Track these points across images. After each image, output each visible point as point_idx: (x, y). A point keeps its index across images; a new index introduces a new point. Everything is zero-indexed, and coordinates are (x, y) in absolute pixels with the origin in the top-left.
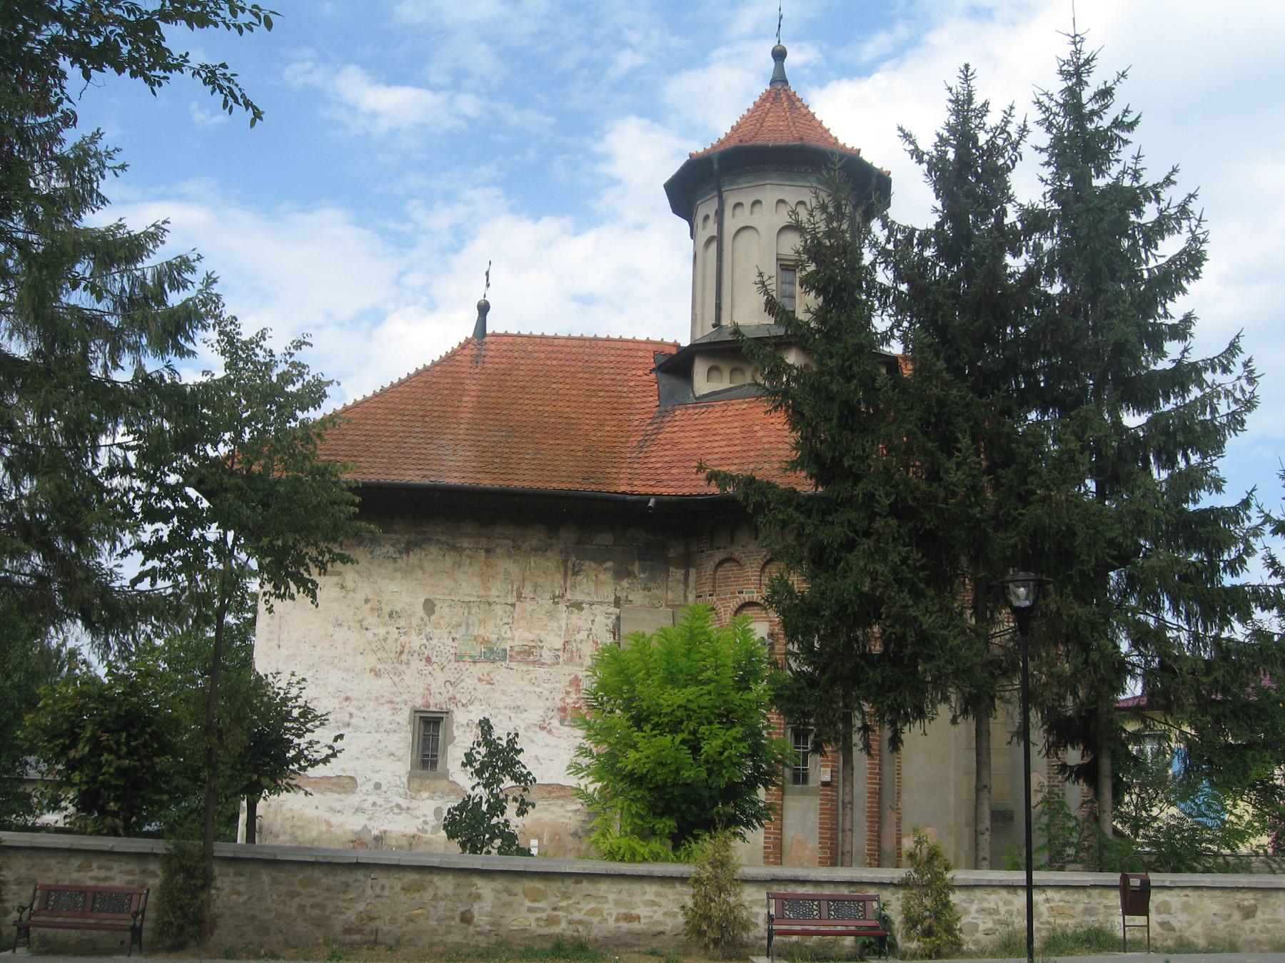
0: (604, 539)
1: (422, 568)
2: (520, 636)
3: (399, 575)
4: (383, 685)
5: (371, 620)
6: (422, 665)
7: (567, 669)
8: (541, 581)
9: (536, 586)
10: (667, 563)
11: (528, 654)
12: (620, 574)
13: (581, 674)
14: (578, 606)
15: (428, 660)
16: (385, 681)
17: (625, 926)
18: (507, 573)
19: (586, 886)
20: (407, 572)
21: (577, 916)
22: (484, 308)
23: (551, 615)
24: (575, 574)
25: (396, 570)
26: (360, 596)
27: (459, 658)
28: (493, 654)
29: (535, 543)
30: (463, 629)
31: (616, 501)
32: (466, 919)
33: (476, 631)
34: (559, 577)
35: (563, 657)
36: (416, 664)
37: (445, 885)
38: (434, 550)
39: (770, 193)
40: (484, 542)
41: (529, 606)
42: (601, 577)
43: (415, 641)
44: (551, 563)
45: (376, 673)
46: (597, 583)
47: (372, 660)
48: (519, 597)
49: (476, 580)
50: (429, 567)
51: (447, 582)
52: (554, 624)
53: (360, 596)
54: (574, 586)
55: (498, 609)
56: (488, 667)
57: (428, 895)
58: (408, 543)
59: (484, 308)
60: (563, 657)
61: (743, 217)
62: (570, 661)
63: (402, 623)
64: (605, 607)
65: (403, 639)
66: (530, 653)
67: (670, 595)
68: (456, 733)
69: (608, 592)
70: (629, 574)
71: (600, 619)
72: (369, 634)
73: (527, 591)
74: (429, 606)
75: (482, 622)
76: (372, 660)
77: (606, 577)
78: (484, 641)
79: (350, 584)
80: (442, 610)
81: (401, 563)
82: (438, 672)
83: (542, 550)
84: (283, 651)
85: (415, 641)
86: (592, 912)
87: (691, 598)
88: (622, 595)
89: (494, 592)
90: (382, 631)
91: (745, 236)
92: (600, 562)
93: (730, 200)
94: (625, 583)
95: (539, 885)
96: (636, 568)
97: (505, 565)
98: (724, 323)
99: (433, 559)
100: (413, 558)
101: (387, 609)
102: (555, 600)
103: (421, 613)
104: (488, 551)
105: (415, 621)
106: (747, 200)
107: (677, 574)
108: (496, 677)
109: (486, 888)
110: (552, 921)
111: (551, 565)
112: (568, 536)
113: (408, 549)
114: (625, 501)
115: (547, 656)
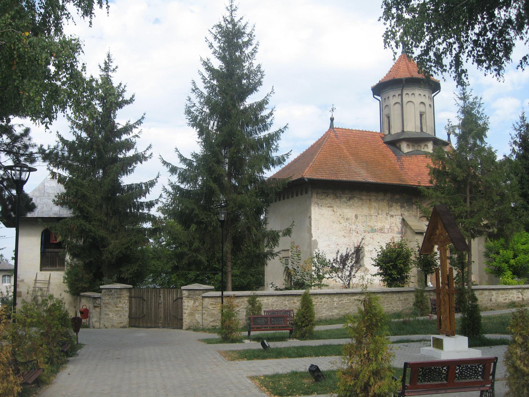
0: (397, 197)
1: (354, 205)
2: (379, 225)
3: (348, 207)
4: (346, 240)
5: (342, 221)
6: (356, 234)
7: (391, 234)
8: (383, 209)
9: (382, 210)
10: (412, 204)
11: (381, 230)
12: (402, 207)
13: (395, 235)
14: (392, 216)
15: (357, 232)
16: (347, 239)
17: (518, 299)
18: (375, 207)
19: (511, 291)
20: (350, 206)
21: (510, 298)
22: (332, 120)
23: (386, 219)
24: (391, 207)
25: (347, 206)
26: (338, 214)
27: (365, 232)
28: (373, 231)
29: (381, 198)
30: (365, 223)
31: (410, 187)
32: (491, 300)
33: (369, 224)
34: (387, 208)
35: (390, 231)
36: (355, 234)
37: (486, 293)
38: (356, 200)
39: (417, 92)
40: (368, 197)
41: (380, 216)
42: (398, 208)
43: (354, 227)
44: (385, 203)
45: (345, 237)
46: (397, 210)
47: (343, 233)
48: (378, 214)
49: (367, 209)
50: (356, 205)
51: (361, 210)
52: (387, 222)
53: (338, 214)
54: (391, 210)
55: (373, 217)
56: (372, 234)
57: (484, 296)
58: (350, 198)
59: (332, 120)
60: (390, 231)
61: (411, 98)
62: (391, 232)
63: (350, 222)
64: (399, 217)
65: (351, 226)
66: (382, 230)
67: (414, 213)
68: (366, 253)
69: (399, 212)
70: (404, 207)
71: (398, 220)
72: (342, 225)
73: (380, 212)
74: (356, 216)
75: (370, 221)
76: (343, 233)
77: (398, 208)
78: (371, 227)
79: (335, 210)
80: (360, 217)
81: (348, 204)
82: (360, 236)
83: (382, 200)
84: (319, 231)
85: (354, 227)
86: (512, 297)
87: (418, 214)
88: (402, 213)
89: (372, 212)
90: (345, 224)
91: (410, 104)
92: (397, 204)
93: (405, 92)
94: (403, 210)
95: (503, 291)
96: (405, 205)
97: (374, 204)
98: (405, 130)
99: (356, 202)
100: (351, 202)
101: (346, 218)
102: (387, 214)
103: (354, 218)
104: (370, 200)
105: (353, 221)
106: (410, 93)
107: (415, 207)
108: (374, 237)
109: (494, 293)
110: (505, 299)
111: (385, 204)
112: (389, 196)
113: (350, 199)
114: (413, 187)
115: (386, 231)
